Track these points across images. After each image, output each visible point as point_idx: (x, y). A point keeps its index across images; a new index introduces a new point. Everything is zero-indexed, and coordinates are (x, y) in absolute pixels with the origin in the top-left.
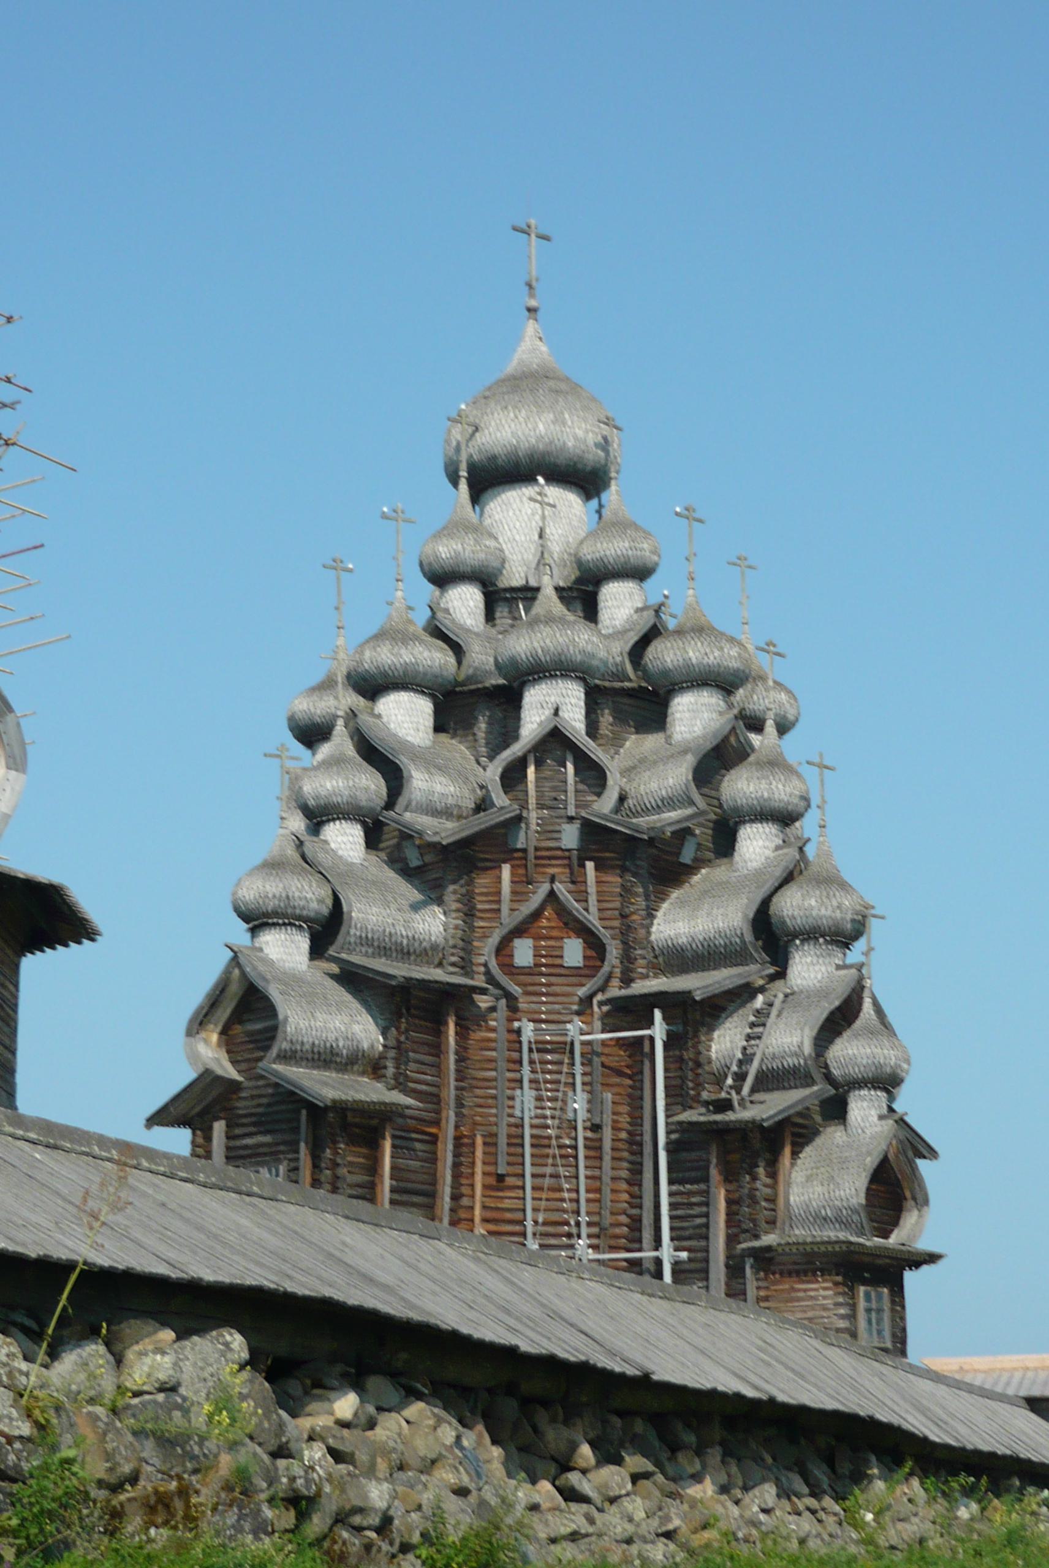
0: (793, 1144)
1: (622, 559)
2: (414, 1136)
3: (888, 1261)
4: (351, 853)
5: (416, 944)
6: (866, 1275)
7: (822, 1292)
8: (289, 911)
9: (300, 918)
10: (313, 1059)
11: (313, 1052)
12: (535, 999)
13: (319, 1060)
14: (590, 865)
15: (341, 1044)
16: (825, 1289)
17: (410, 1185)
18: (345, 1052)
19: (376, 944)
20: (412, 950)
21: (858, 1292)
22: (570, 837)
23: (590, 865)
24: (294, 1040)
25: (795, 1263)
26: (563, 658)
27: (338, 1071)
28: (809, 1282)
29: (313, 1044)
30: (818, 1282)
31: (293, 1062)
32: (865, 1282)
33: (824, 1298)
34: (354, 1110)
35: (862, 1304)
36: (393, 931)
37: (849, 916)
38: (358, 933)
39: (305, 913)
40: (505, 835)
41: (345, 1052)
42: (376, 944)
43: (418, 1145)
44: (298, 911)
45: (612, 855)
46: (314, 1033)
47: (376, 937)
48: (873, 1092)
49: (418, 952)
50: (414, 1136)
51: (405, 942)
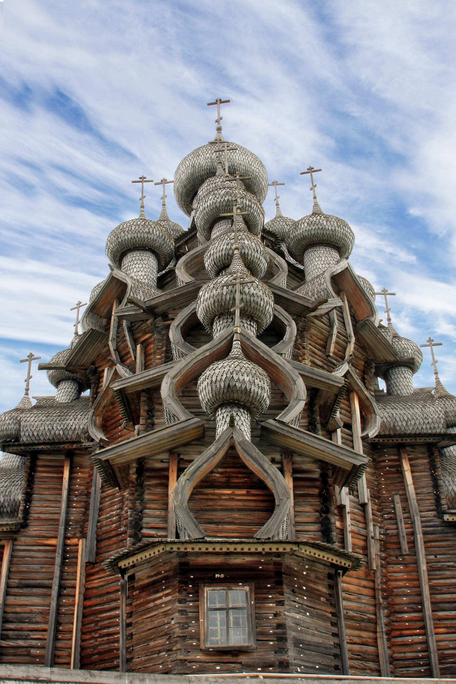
3: (248, 559)
4: (63, 398)
5: (70, 433)
6: (217, 575)
7: (165, 599)
17: (31, 582)
25: (149, 577)
26: (120, 240)
30: (163, 590)
32: (213, 582)
33: (166, 603)
38: (27, 434)
41: (6, 504)
44: (5, 433)
47: (40, 433)
51: (61, 432)
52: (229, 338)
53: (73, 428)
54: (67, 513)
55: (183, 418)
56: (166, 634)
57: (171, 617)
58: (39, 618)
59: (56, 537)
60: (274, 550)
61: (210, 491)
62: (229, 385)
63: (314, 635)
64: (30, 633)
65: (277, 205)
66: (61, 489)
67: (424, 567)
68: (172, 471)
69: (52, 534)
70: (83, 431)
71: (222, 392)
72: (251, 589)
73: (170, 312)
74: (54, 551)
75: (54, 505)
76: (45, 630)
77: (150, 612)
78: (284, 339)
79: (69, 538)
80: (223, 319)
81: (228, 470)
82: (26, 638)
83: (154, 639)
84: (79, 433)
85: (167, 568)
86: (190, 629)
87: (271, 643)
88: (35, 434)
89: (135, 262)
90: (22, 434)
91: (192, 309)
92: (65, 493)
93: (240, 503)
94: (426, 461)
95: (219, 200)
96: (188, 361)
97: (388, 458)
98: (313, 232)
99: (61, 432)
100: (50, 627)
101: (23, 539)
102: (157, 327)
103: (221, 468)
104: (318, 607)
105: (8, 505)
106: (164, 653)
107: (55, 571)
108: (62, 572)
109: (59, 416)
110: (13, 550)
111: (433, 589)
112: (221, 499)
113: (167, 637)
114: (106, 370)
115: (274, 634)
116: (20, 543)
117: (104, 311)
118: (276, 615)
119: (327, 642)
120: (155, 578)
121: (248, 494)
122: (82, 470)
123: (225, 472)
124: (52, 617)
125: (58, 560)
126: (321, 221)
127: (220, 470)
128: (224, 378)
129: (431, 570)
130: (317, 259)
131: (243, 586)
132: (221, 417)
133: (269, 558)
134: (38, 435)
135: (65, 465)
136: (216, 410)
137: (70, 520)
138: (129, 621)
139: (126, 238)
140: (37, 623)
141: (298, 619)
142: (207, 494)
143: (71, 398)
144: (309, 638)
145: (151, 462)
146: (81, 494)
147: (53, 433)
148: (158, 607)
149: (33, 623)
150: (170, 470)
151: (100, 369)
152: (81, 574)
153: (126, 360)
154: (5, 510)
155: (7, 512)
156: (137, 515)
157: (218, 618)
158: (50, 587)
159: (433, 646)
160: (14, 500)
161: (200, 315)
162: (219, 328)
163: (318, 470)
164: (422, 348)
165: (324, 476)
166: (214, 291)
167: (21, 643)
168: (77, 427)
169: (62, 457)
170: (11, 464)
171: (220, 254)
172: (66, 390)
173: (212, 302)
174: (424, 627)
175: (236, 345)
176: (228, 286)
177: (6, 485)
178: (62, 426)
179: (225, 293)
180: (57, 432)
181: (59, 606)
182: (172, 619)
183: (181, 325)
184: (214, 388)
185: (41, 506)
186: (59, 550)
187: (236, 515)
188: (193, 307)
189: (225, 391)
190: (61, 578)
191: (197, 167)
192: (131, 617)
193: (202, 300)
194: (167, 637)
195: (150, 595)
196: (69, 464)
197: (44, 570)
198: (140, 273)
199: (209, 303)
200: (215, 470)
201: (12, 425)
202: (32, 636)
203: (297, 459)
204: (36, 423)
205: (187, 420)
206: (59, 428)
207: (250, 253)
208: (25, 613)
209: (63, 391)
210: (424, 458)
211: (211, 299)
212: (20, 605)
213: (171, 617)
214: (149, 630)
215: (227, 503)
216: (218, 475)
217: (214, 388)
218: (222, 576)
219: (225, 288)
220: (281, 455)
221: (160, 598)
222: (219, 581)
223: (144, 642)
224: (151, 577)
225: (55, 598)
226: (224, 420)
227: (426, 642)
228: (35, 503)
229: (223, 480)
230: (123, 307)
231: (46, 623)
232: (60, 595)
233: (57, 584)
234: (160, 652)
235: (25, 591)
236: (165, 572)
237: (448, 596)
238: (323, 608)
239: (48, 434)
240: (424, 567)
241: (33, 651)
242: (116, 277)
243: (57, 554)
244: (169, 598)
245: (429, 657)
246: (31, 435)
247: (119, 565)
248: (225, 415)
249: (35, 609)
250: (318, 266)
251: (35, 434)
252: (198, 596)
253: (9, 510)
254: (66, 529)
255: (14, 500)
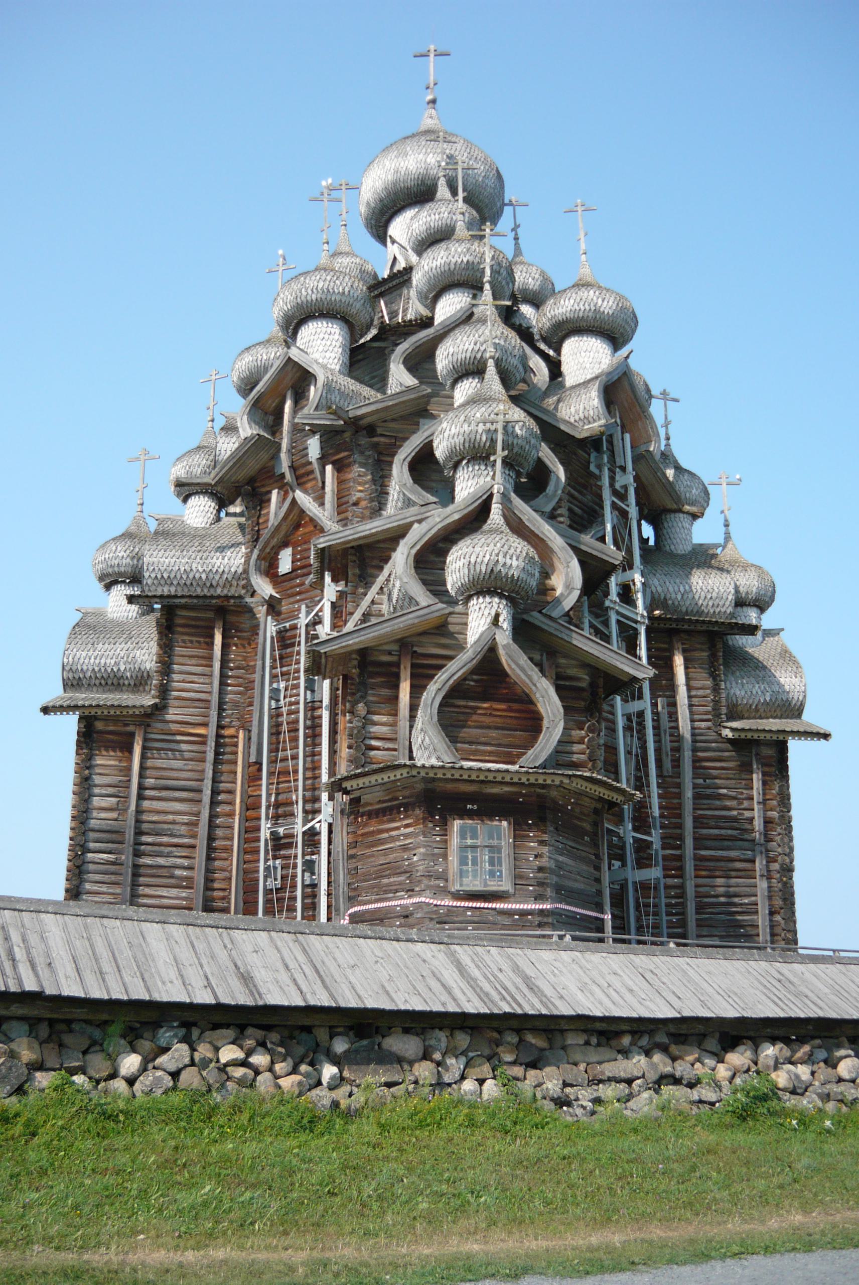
0: (413, 676)
1: (424, 227)
2: (179, 738)
3: (507, 789)
4: (197, 520)
7: (403, 831)
8: (110, 570)
9: (120, 574)
10: (100, 684)
11: (96, 677)
12: (292, 600)
13: (107, 684)
14: (329, 468)
15: (122, 669)
16: (407, 826)
18: (128, 674)
19: (175, 582)
20: (214, 583)
21: (453, 825)
22: (314, 448)
23: (329, 468)
24: (74, 668)
25: (380, 802)
27: (133, 692)
28: (394, 821)
29: (93, 670)
30: (401, 819)
31: (83, 689)
32: (464, 814)
33: (406, 836)
34: (106, 719)
35: (455, 840)
36: (188, 569)
37: (481, 427)
38: (153, 575)
39: (122, 569)
40: (273, 467)
41: (128, 674)
42: (175, 582)
43: (184, 747)
44: (116, 569)
45: (346, 454)
46: (92, 661)
47: (172, 576)
48: (481, 600)
49: (221, 583)
50: (179, 738)
51: (204, 576)
52: (484, 497)
53: (221, 570)
54: (222, 693)
55: (423, 604)
56: (406, 872)
57: (414, 852)
58: (183, 829)
59: (205, 725)
60: (541, 781)
61: (462, 703)
62: (492, 570)
63: (576, 880)
64: (174, 849)
65: (516, 239)
66: (210, 658)
67: (689, 794)
68: (405, 668)
69: (200, 719)
70: (236, 576)
71: (481, 578)
72: (509, 824)
73: (379, 425)
74: (204, 743)
75: (201, 680)
76: (193, 847)
77: (382, 844)
78: (547, 491)
79: (223, 727)
80: (474, 465)
81: (484, 677)
82: (168, 855)
83: (388, 876)
84: (230, 579)
85: (407, 793)
86: (436, 867)
87: (531, 888)
88: (166, 576)
89: (321, 336)
90: (146, 575)
91: (424, 437)
92: (217, 665)
93: (498, 720)
94: (706, 654)
95: (454, 261)
96: (432, 524)
97: (656, 646)
98: (581, 314)
99: (204, 576)
100: (201, 842)
101: (159, 725)
102: (359, 445)
103: (476, 674)
104: (580, 848)
105: (131, 676)
106: (403, 893)
107: (207, 770)
108: (215, 772)
109: (199, 551)
110: (145, 740)
111: (699, 822)
112: (475, 713)
113: (408, 875)
114: (275, 493)
115: (534, 878)
116: (155, 731)
117: (272, 404)
118: (536, 856)
119: (588, 888)
120: (389, 804)
121: (510, 710)
122: (239, 634)
123: (482, 680)
124: (203, 830)
125: (210, 756)
126: (595, 299)
127: (475, 677)
128: (486, 560)
129: (697, 797)
130: (583, 354)
131: (500, 820)
132: (477, 608)
133: (533, 790)
134: (169, 577)
135: (217, 626)
136: (469, 598)
137: (226, 703)
138: (351, 852)
139: (309, 298)
140: (182, 836)
141: (562, 862)
142: (459, 707)
143: (210, 521)
144: (570, 884)
145: (376, 653)
146: (238, 668)
147: (191, 576)
148: (393, 839)
149: (175, 836)
150: (402, 667)
151: (264, 490)
152: (243, 776)
153: (305, 483)
154: (126, 682)
155: (129, 684)
156: (361, 721)
157: (470, 857)
158: (200, 791)
159: (690, 891)
160: (140, 669)
161: (440, 452)
162: (467, 477)
163: (586, 677)
164: (710, 488)
165: (593, 685)
166: (466, 426)
167: (161, 861)
168: (226, 570)
169: (210, 615)
170: (126, 614)
171: (463, 356)
172: (202, 508)
173: (462, 442)
174: (681, 869)
175: (496, 509)
176: (485, 423)
177: (126, 647)
178: (205, 567)
179: (480, 431)
180: (197, 576)
181: (212, 816)
182: (415, 855)
183: (409, 459)
184: (472, 572)
185: (183, 681)
186: (211, 743)
187: (494, 733)
188: (426, 434)
189: (487, 577)
190: (214, 781)
191: (403, 173)
192: (355, 847)
193: (446, 435)
194: (408, 875)
195: (383, 822)
196: (221, 626)
197: (190, 767)
198: (328, 355)
199: (457, 441)
200: (469, 677)
201: (128, 560)
202: (176, 854)
203: (562, 661)
204: (167, 561)
205: (429, 606)
206: (201, 570)
207: (504, 358)
208: (165, 823)
209: (197, 508)
210: (702, 650)
211: (460, 437)
212: (158, 812)
213: (414, 852)
214: (382, 865)
215: (482, 719)
216: (472, 683)
217: (472, 572)
218: (475, 807)
219: (481, 425)
220: (542, 655)
221: (398, 828)
222: (471, 815)
223: (375, 879)
224: (384, 802)
225: (208, 807)
226: (481, 613)
227: (682, 887)
228: (175, 677)
229: (479, 690)
230: (311, 412)
231: (194, 836)
232: (214, 803)
233: (210, 788)
234: (397, 891)
235: (164, 794)
236: (404, 798)
237: (716, 832)
238: (587, 849)
239: (184, 577)
240: (689, 794)
241: (178, 872)
242: (296, 360)
243: (208, 749)
244: (411, 830)
245: (683, 905)
246: (159, 576)
247: (344, 786)
248: (483, 606)
249: (179, 818)
250: (583, 366)
251: (166, 576)
252: (446, 830)
253: (132, 683)
254: (220, 717)
255: (140, 669)
